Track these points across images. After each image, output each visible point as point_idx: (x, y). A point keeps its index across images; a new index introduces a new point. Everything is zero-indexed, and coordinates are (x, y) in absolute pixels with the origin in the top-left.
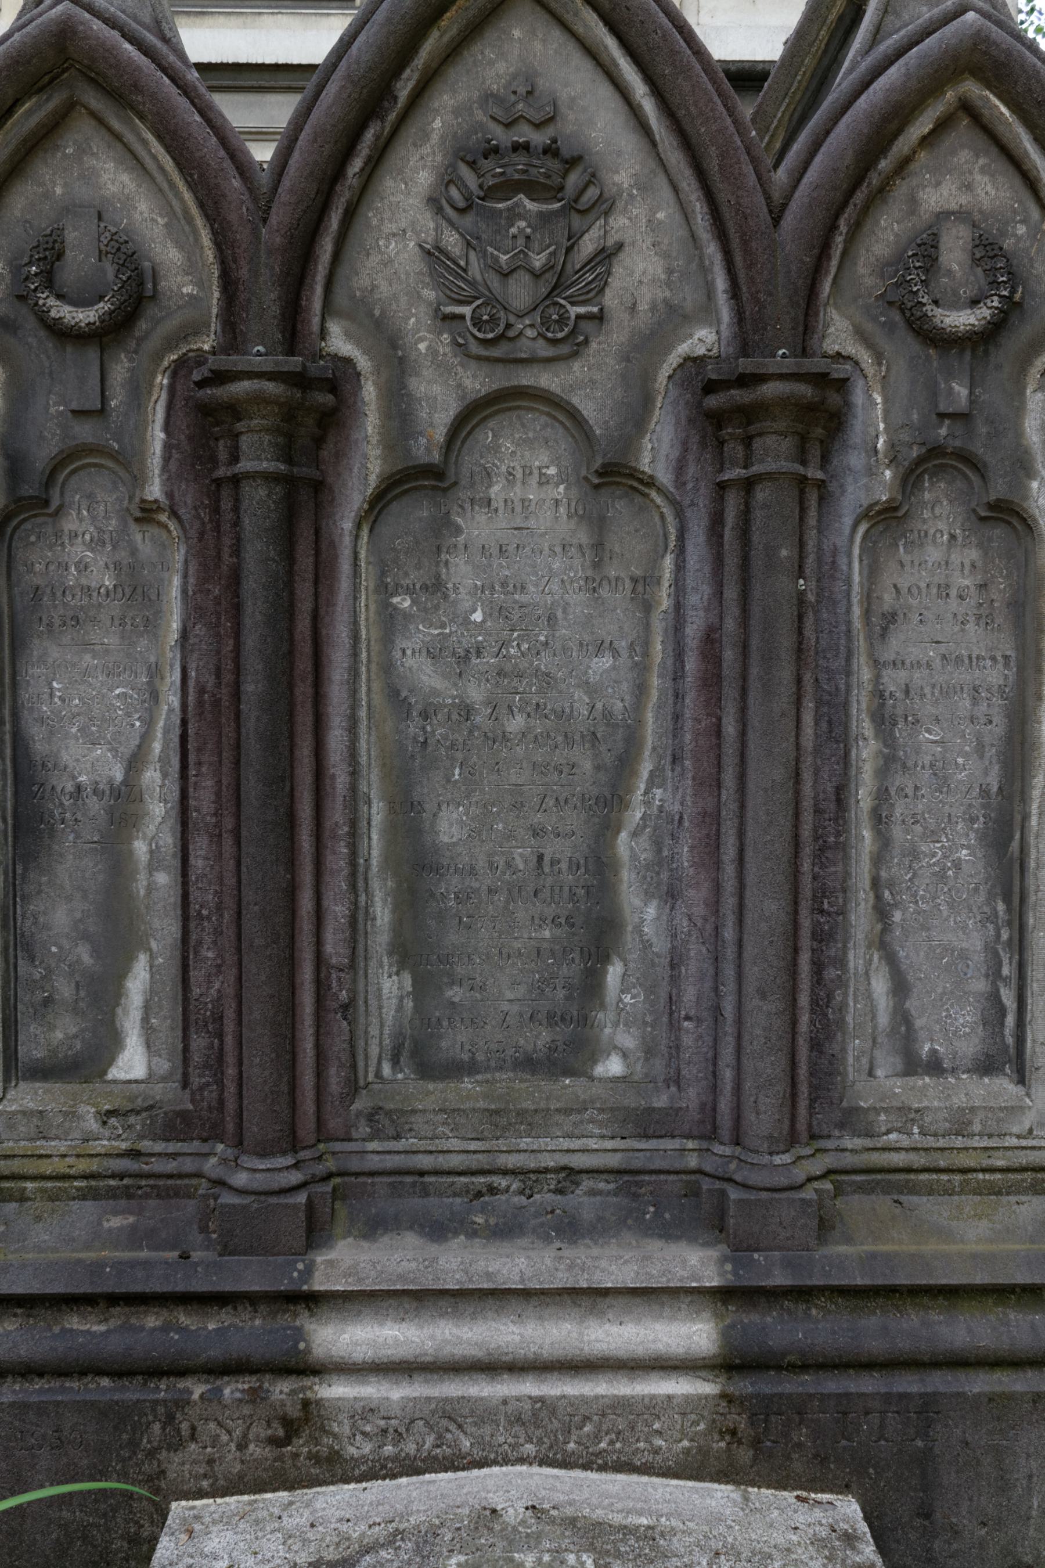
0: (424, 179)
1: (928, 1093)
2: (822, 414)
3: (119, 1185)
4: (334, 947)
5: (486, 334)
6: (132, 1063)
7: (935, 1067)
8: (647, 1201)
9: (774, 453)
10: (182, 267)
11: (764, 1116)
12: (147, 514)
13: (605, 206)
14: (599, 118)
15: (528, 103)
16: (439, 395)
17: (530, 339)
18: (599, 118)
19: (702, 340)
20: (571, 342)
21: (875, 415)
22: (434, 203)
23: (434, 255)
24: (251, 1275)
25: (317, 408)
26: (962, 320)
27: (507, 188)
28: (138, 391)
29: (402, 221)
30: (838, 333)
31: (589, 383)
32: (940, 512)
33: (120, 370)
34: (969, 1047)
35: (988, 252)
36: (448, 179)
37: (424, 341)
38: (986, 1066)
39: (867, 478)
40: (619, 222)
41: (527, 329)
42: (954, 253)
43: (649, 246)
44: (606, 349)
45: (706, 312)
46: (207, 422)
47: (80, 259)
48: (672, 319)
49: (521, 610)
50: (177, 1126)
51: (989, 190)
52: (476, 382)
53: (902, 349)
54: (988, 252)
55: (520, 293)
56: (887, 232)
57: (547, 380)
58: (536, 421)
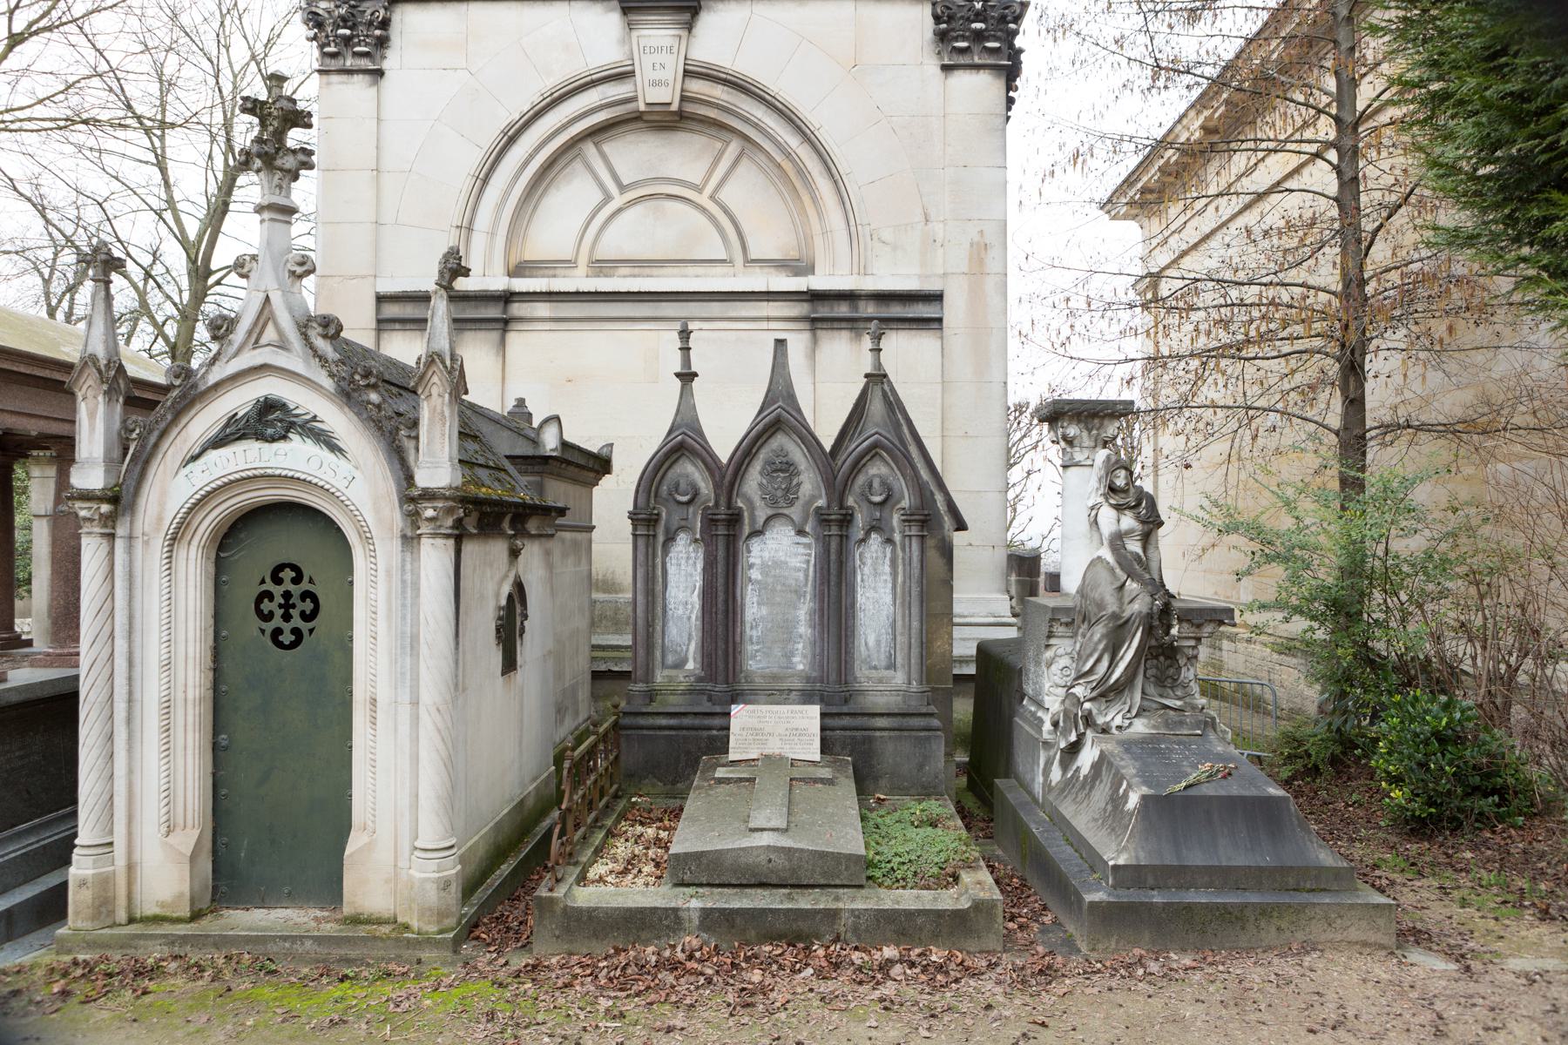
0: (758, 468)
1: (874, 673)
2: (846, 520)
3: (690, 691)
4: (738, 639)
5: (773, 502)
6: (690, 665)
7: (875, 668)
8: (807, 698)
9: (835, 530)
10: (706, 487)
11: (833, 677)
12: (696, 541)
13: (798, 474)
14: (798, 454)
15: (782, 452)
16: (762, 514)
17: (782, 504)
18: (798, 454)
19: (821, 502)
20: (791, 503)
21: (860, 520)
22: (761, 473)
23: (761, 485)
24: (718, 709)
25: (734, 519)
26: (877, 499)
27: (776, 471)
28: (695, 514)
29: (753, 481)
30: (850, 501)
31: (795, 512)
32: (875, 539)
33: (691, 510)
34: (884, 663)
35: (884, 483)
36: (763, 468)
37: (758, 503)
38: (888, 668)
39: (858, 531)
40: (802, 477)
41: (781, 501)
42: (876, 484)
43: (809, 483)
44: (798, 505)
45: (820, 497)
46: (710, 522)
47: (683, 486)
48: (813, 498)
49: (780, 555)
50: (700, 679)
51: (884, 470)
52: (770, 512)
53: (865, 505)
54: (884, 483)
55: (779, 493)
56: (861, 480)
57: (786, 511)
58: (783, 520)
